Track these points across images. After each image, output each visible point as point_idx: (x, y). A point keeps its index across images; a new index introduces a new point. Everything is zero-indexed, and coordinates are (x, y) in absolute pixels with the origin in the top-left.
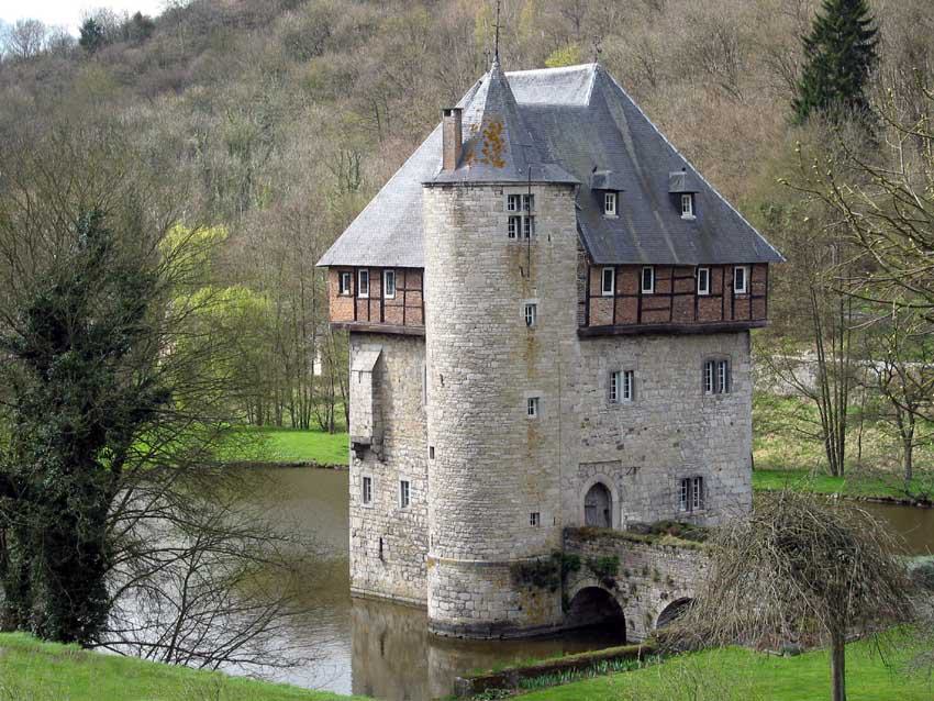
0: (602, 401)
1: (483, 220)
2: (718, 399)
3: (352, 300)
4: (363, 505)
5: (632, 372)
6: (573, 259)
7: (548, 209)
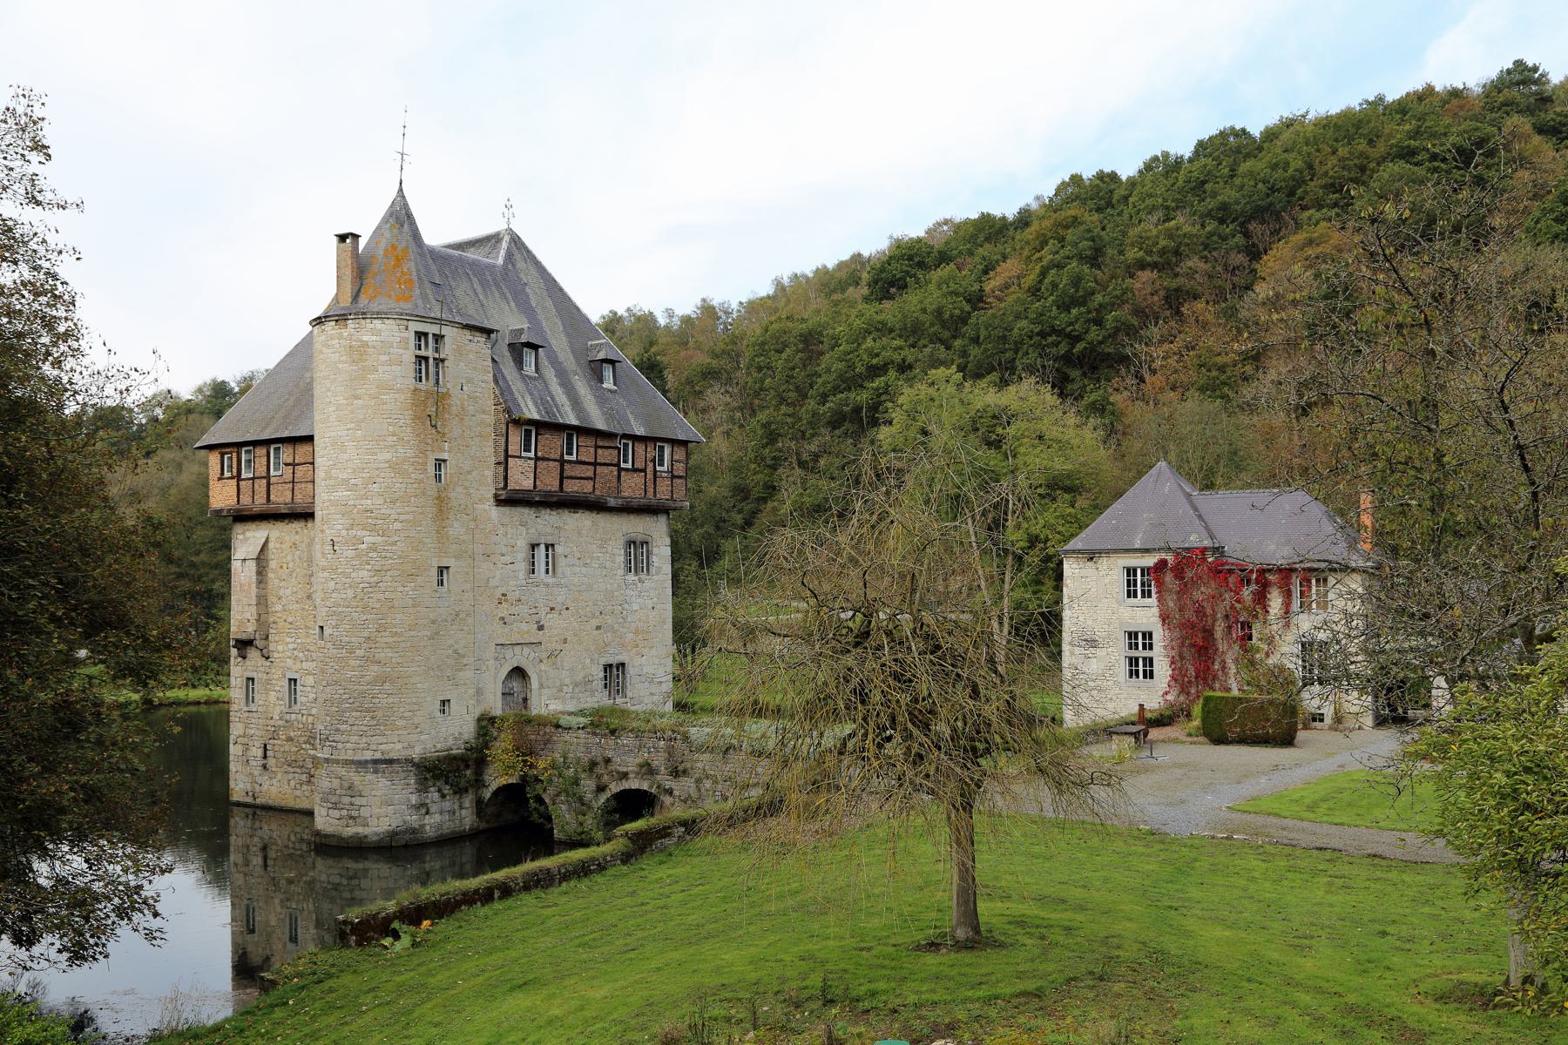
0: (522, 575)
1: (384, 358)
3: (234, 482)
4: (246, 709)
5: (553, 545)
7: (461, 354)
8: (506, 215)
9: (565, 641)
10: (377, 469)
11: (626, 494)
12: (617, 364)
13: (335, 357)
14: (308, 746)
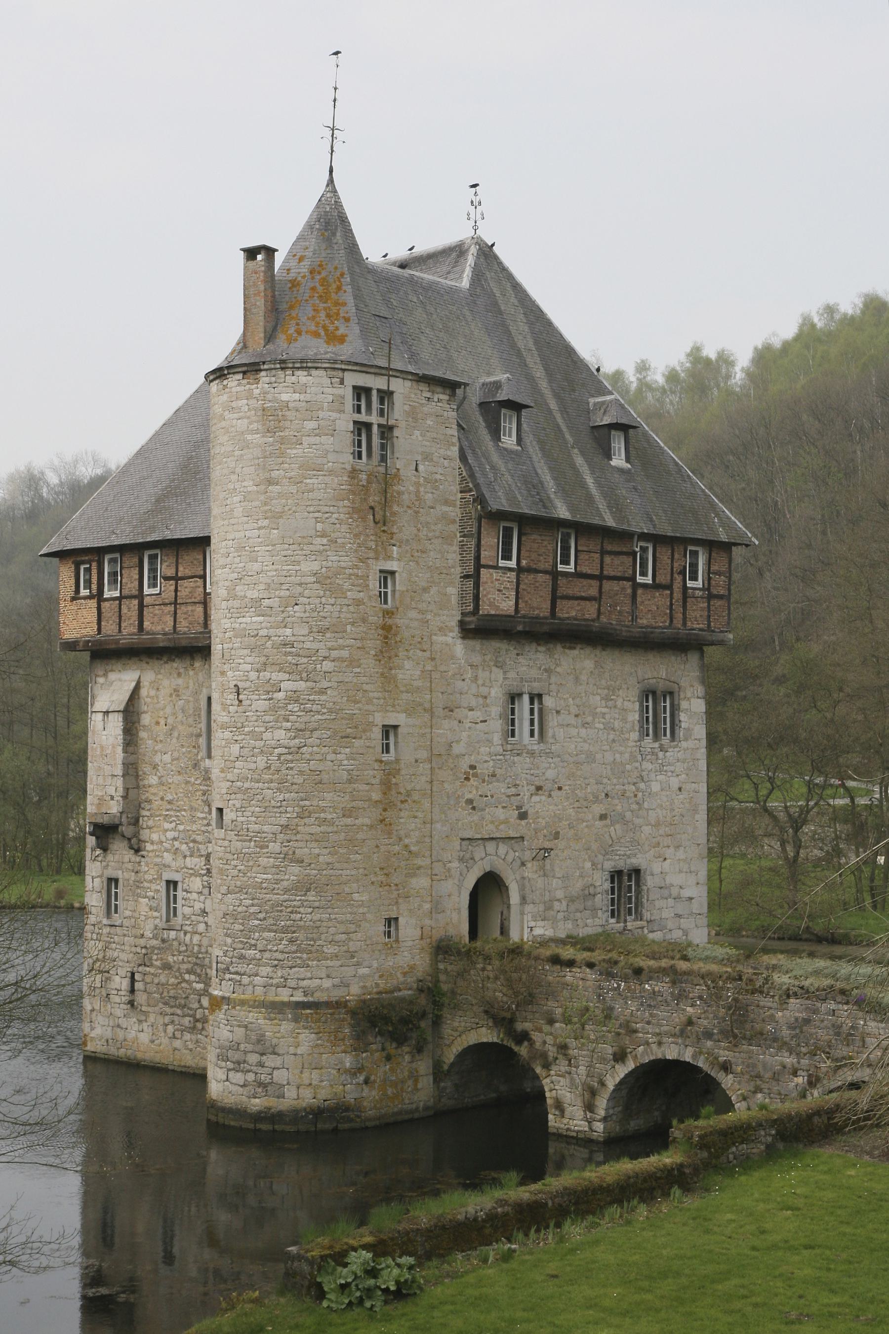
0: (497, 738)
1: (311, 425)
2: (662, 748)
3: (93, 603)
4: (105, 921)
5: (540, 696)
6: (454, 506)
7: (416, 420)
8: (472, 216)
9: (556, 836)
10: (300, 584)
11: (644, 622)
12: (631, 431)
13: (242, 424)
14: (193, 977)
